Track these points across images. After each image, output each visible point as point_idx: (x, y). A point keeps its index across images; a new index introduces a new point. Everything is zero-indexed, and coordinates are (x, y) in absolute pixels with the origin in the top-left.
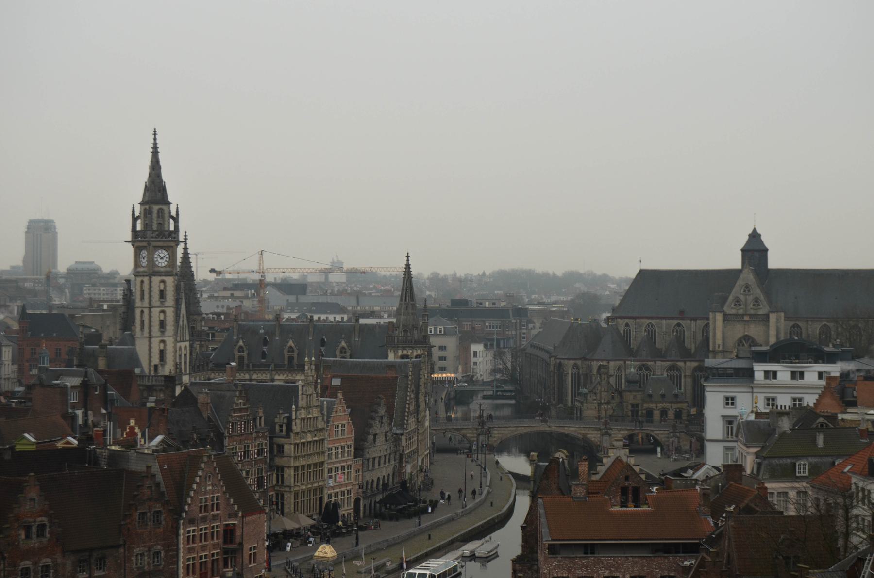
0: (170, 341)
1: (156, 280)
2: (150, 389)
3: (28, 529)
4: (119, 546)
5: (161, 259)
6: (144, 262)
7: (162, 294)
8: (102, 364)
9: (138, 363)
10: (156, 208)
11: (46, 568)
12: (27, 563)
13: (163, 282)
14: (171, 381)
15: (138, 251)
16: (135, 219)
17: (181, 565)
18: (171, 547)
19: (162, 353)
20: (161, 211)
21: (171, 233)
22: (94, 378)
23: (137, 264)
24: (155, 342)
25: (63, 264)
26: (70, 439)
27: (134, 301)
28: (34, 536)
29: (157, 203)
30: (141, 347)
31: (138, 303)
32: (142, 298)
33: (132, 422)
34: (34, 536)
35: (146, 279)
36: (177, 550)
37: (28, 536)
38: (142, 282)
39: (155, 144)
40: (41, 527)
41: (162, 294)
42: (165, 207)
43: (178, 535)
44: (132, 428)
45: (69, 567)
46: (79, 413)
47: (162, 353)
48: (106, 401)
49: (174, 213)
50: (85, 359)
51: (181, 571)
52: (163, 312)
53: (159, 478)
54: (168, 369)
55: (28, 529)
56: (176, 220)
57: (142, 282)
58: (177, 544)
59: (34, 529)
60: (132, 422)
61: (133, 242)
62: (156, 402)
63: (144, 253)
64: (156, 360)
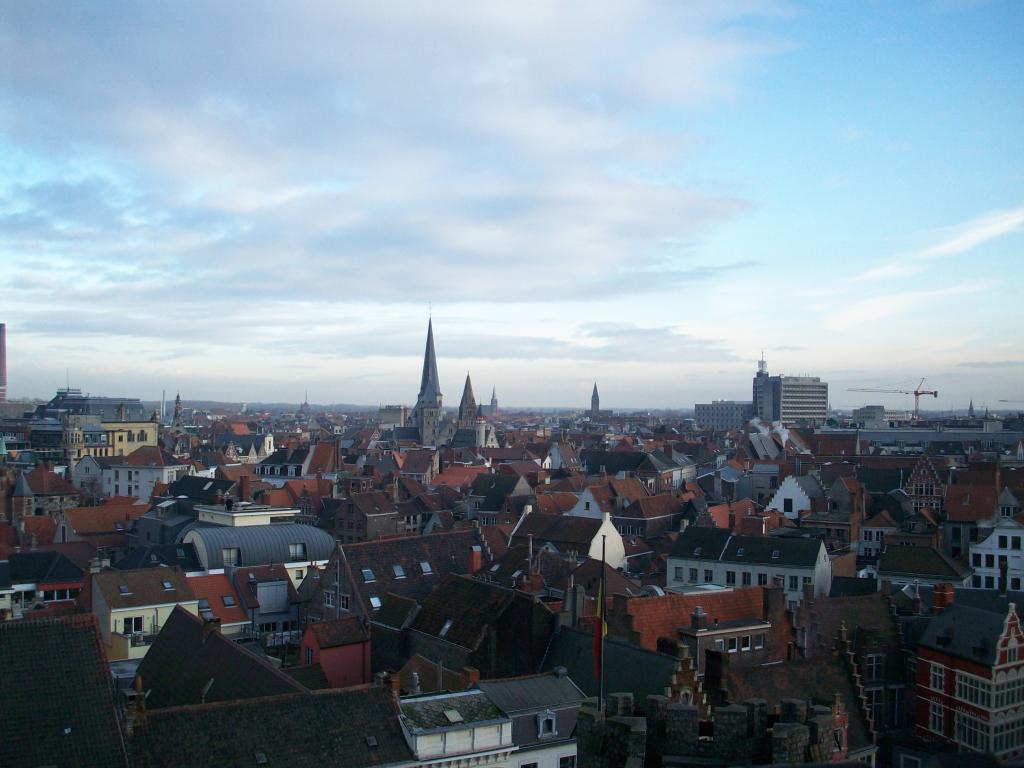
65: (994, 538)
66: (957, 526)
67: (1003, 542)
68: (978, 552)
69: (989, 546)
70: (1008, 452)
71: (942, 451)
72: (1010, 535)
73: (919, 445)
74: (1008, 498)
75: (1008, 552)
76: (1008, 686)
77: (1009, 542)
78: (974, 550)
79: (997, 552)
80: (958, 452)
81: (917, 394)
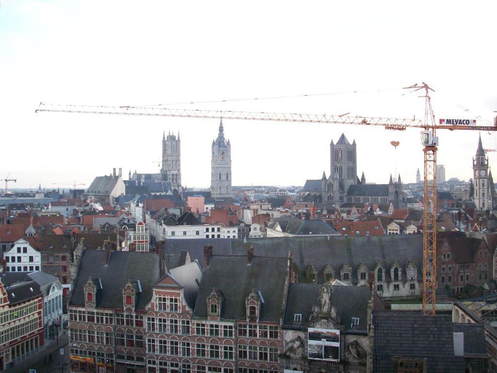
0: (486, 200)
1: (481, 180)
2: (480, 215)
3: (445, 255)
4: (473, 262)
5: (483, 173)
6: (477, 174)
7: (483, 185)
8: (464, 207)
9: (475, 207)
10: (481, 157)
11: (450, 268)
12: (444, 266)
13: (483, 181)
14: (488, 212)
15: (475, 171)
16: (474, 161)
17: (494, 270)
18: (491, 264)
19: (483, 204)
20: (482, 158)
21: (486, 165)
22: (462, 211)
23: (475, 175)
24: (481, 200)
25: (447, 179)
26: (456, 229)
27: (474, 187)
28: (446, 258)
29: (481, 155)
30: (476, 202)
31: (475, 188)
32: (477, 186)
33: (476, 224)
34: (446, 258)
35: (478, 180)
36: (493, 265)
37: (444, 258)
38: (476, 181)
39: (480, 138)
40: (449, 255)
41: (483, 185)
42: (483, 156)
43: (492, 260)
44: (476, 226)
45: (457, 267)
46: (457, 222)
47: (483, 204)
48: (467, 218)
49: (486, 159)
50: (459, 206)
51: (494, 272)
52: (483, 190)
53: (486, 241)
54: (485, 209)
55: (445, 255)
56: (487, 161)
57: (476, 181)
58: (493, 263)
59: (446, 255)
60: (476, 224)
61: (473, 168)
62: (482, 219)
63: (477, 172)
64: (481, 206)
65: (15, 248)
66: (4, 244)
67: (19, 250)
68: (8, 255)
69: (13, 253)
70: (45, 208)
71: (15, 208)
72: (22, 246)
73: (3, 206)
74: (31, 230)
75: (22, 255)
76: (5, 313)
77: (22, 250)
78: (6, 255)
79: (16, 255)
80: (22, 209)
81: (6, 180)
